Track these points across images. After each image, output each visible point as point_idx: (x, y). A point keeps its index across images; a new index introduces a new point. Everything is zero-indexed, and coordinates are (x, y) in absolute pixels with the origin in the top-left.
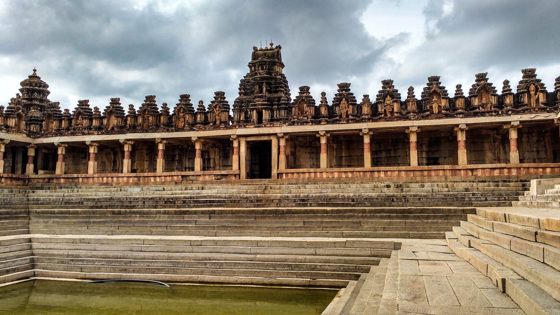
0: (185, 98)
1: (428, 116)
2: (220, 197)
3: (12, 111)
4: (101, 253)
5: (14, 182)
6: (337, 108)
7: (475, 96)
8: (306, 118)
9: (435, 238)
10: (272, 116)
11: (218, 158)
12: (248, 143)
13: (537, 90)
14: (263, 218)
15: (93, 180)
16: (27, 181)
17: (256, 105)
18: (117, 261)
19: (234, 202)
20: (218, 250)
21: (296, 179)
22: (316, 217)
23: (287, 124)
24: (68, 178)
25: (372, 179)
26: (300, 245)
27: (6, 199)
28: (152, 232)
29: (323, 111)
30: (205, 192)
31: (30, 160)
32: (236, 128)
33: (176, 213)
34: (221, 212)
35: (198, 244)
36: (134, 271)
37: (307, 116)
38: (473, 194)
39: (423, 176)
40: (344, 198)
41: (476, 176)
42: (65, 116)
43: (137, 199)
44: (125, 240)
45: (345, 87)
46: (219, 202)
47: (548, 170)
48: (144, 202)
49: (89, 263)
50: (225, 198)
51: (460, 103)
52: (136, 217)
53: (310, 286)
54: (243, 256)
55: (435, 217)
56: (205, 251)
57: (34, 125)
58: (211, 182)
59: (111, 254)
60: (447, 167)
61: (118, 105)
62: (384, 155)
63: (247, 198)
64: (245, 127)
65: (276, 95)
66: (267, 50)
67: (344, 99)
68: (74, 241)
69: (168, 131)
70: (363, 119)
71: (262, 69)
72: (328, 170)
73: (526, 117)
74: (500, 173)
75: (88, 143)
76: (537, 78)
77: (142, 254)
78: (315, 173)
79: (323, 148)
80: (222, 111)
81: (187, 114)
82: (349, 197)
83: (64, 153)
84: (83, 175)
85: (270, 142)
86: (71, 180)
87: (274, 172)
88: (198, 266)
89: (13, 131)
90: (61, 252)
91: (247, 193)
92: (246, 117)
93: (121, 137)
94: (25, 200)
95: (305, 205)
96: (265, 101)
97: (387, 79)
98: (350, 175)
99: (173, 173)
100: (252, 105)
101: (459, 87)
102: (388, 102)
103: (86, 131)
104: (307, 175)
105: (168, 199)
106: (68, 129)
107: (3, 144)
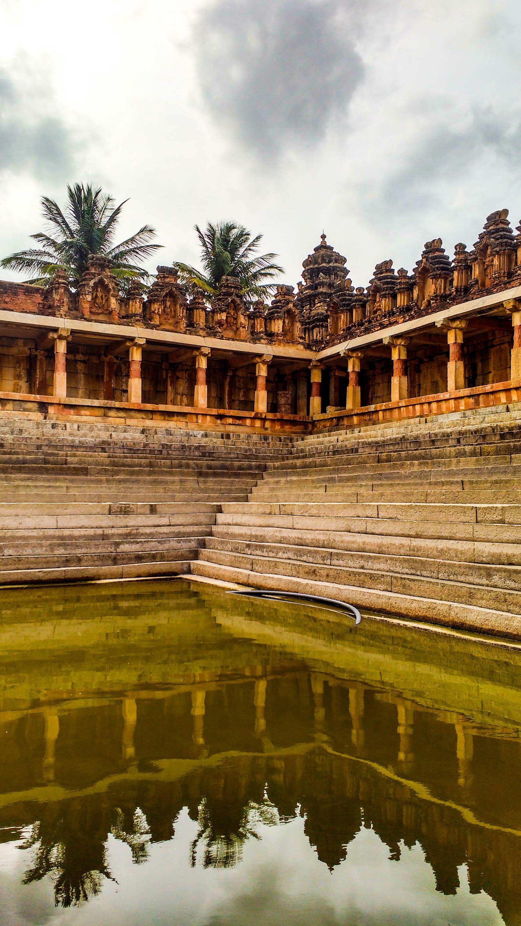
3: (277, 307)
5: (287, 428)
15: (400, 413)
16: (310, 426)
24: (363, 414)
27: (250, 450)
31: (315, 389)
42: (356, 301)
49: (271, 554)
57: (317, 329)
61: (437, 254)
75: (386, 342)
83: (357, 369)
84: (384, 406)
86: (367, 417)
88: (471, 579)
89: (280, 341)
93: (438, 318)
94: (285, 452)
103: (385, 321)
106: (361, 324)
107: (264, 362)
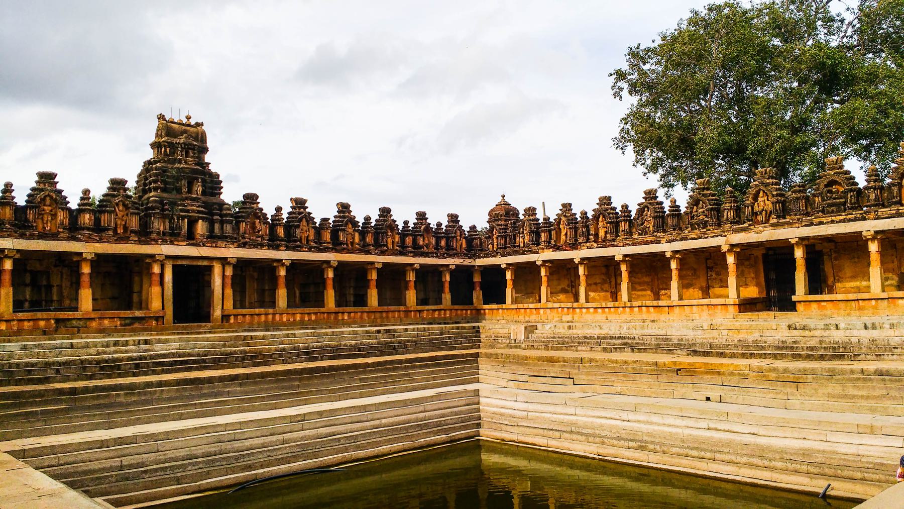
0: (47, 178)
1: (386, 251)
2: (190, 355)
4: (183, 453)
6: (298, 231)
7: (421, 235)
8: (260, 239)
9: (472, 383)
10: (211, 229)
11: (68, 284)
12: (175, 268)
13: (461, 235)
14: (309, 379)
17: (188, 211)
18: (224, 458)
19: (219, 362)
20: (332, 423)
21: (249, 323)
22: (364, 372)
23: (236, 245)
25: (337, 323)
26: (405, 403)
28: (182, 414)
29: (281, 232)
30: (158, 349)
32: (156, 242)
33: (178, 382)
34: (248, 376)
35: (300, 419)
36: (262, 467)
37: (262, 236)
38: (449, 338)
39: (381, 317)
40: (351, 348)
41: (423, 319)
43: (32, 365)
44: (196, 429)
45: (299, 204)
46: (195, 362)
47: (469, 312)
48: (58, 371)
50: (198, 355)
51: (409, 240)
52: (118, 395)
53: (452, 441)
54: (368, 424)
55: (458, 363)
56: (318, 425)
58: (116, 330)
59: (199, 451)
60: (402, 308)
62: (312, 289)
63: (231, 353)
64: (172, 243)
65: (213, 200)
66: (183, 125)
67: (304, 220)
68: (103, 444)
69: (22, 236)
70: (327, 248)
71: (187, 155)
72: (290, 311)
73: (458, 261)
74: (439, 314)
76: (460, 223)
77: (247, 443)
78: (274, 314)
79: (282, 282)
80: (132, 214)
81: (63, 209)
82: (351, 345)
85: (210, 269)
87: (217, 313)
90: (107, 464)
91: (224, 346)
92: (171, 228)
95: (316, 359)
96: (201, 207)
97: (344, 201)
98: (313, 317)
99: (39, 315)
100: (182, 211)
101: (406, 223)
102: (351, 231)
104: (263, 318)
105: (98, 362)
